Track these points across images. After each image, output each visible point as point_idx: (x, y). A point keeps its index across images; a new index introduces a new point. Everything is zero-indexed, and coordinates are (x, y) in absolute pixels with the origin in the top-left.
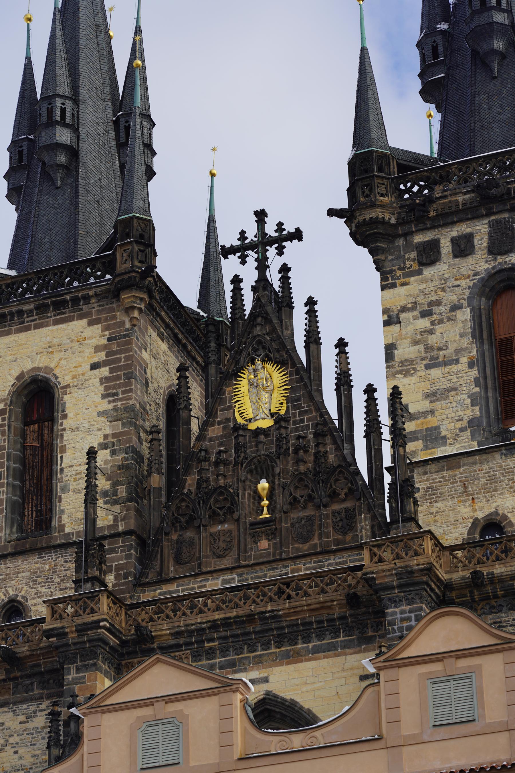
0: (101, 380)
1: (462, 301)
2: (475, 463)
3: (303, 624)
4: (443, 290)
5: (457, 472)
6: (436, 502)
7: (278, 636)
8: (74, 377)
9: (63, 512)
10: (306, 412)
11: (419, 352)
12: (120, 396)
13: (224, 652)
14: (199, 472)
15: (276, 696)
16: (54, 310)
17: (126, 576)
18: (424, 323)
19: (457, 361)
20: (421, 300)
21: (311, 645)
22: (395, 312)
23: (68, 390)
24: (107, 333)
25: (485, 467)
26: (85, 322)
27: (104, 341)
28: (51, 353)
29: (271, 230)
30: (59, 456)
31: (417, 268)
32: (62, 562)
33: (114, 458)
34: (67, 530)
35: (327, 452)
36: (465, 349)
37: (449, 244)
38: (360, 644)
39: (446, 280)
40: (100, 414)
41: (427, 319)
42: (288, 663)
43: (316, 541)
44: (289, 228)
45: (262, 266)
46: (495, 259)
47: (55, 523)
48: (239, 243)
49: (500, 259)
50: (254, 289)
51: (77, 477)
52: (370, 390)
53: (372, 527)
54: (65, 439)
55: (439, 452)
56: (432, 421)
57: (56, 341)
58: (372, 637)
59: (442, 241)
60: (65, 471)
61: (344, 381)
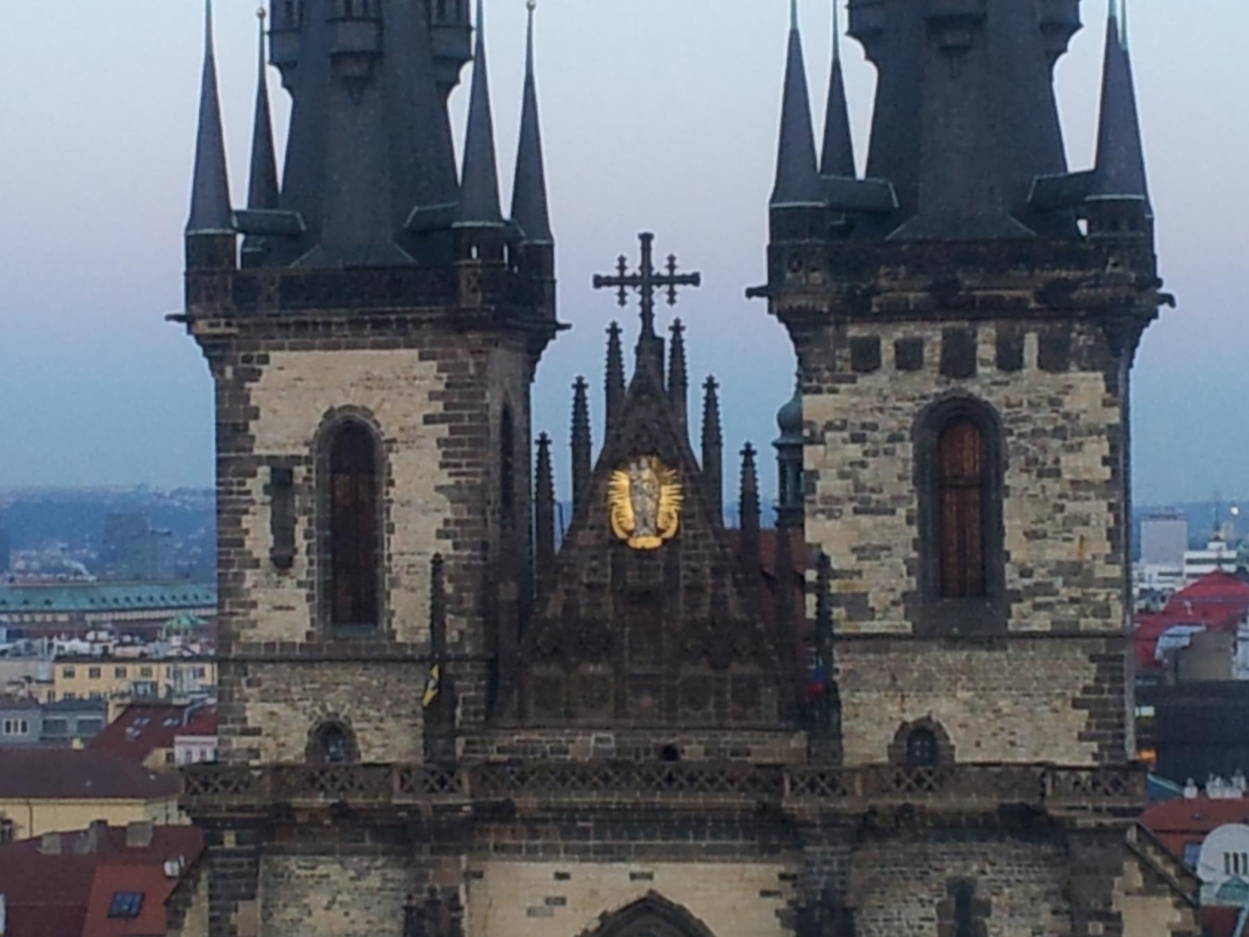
1: (903, 432)
2: (907, 651)
4: (881, 410)
5: (884, 658)
6: (858, 690)
8: (402, 429)
9: (393, 613)
12: (464, 469)
14: (567, 591)
15: (661, 898)
16: (374, 327)
17: (476, 714)
19: (893, 512)
20: (852, 418)
21: (704, 844)
22: (819, 430)
23: (395, 447)
24: (444, 375)
26: (414, 353)
27: (441, 387)
29: (660, 268)
30: (386, 536)
31: (850, 373)
32: (394, 680)
33: (458, 553)
34: (399, 638)
35: (725, 596)
36: (904, 497)
37: (891, 348)
38: (762, 852)
39: (885, 398)
40: (439, 489)
42: (677, 861)
43: (711, 708)
45: (647, 316)
46: (948, 383)
49: (954, 383)
51: (412, 570)
54: (392, 513)
55: (866, 627)
56: (859, 585)
57: (376, 373)
59: (884, 343)
60: (394, 558)
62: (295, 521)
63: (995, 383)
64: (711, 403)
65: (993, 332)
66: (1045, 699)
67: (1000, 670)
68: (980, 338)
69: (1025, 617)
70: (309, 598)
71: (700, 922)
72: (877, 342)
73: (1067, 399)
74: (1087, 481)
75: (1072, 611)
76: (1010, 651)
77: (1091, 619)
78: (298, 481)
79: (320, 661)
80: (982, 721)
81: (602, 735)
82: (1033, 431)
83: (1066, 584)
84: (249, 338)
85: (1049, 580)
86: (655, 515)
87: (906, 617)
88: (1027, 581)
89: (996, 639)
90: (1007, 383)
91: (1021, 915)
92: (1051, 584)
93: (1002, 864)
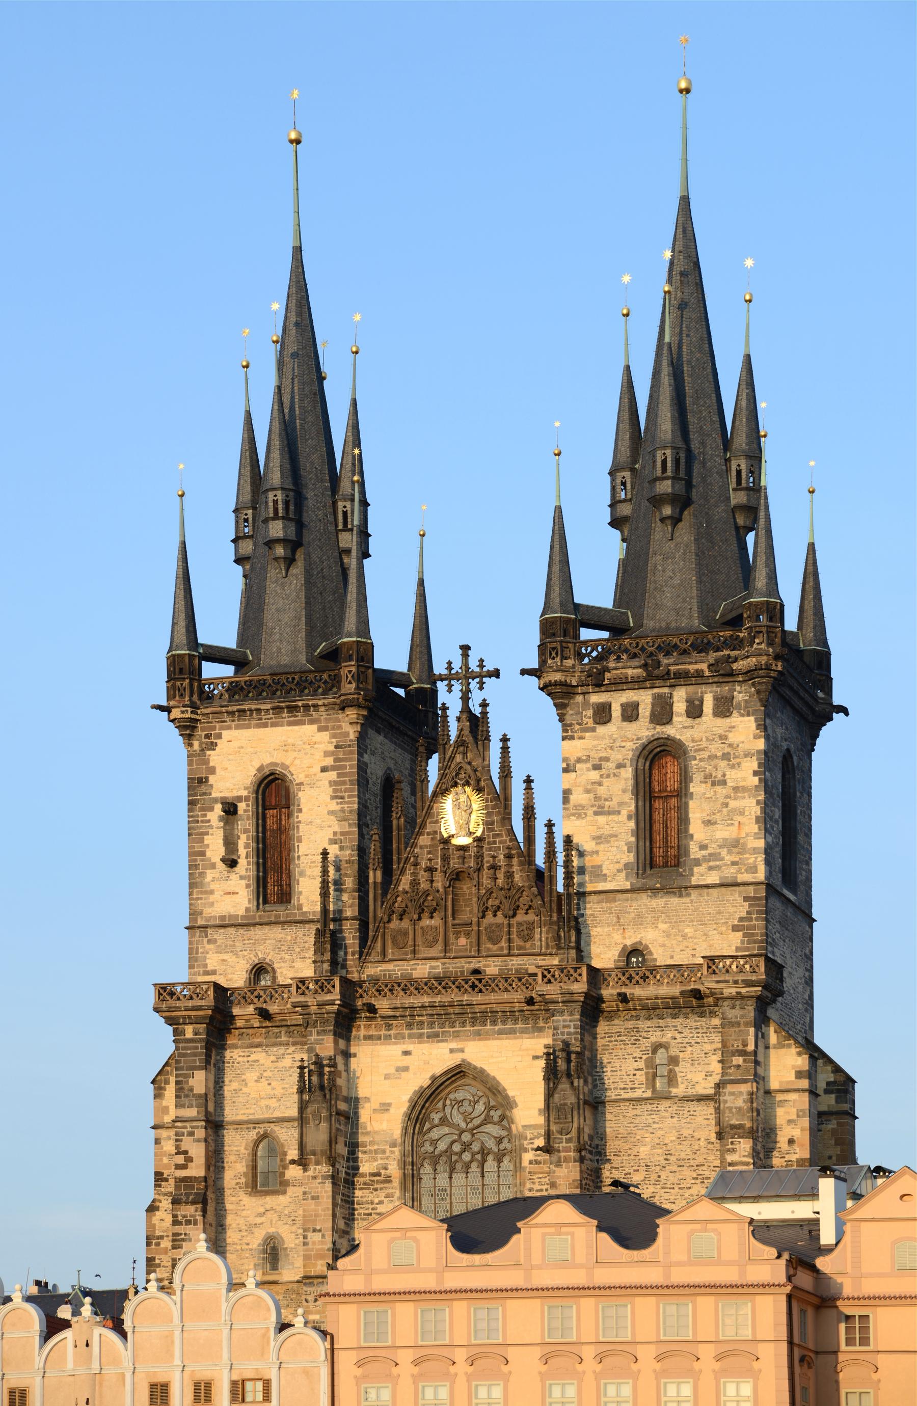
0: (330, 782)
2: (627, 900)
3: (491, 1012)
4: (612, 748)
5: (613, 905)
7: (472, 1018)
8: (307, 776)
9: (301, 893)
10: (498, 835)
11: (590, 800)
12: (346, 800)
13: (431, 1025)
15: (470, 1064)
16: (288, 712)
18: (594, 775)
19: (619, 813)
20: (592, 754)
21: (496, 1028)
22: (572, 762)
24: (334, 740)
25: (634, 904)
26: (315, 727)
28: (287, 751)
33: (342, 852)
34: (305, 909)
37: (619, 708)
38: (533, 1032)
40: (331, 813)
41: (597, 772)
42: (479, 1040)
44: (489, 667)
46: (655, 728)
47: (294, 901)
48: (446, 672)
49: (659, 729)
50: (458, 719)
52: (550, 825)
53: (547, 938)
55: (601, 886)
58: (542, 1027)
59: (613, 705)
61: (529, 813)
62: (239, 838)
63: (685, 727)
64: (505, 750)
65: (684, 693)
66: (715, 926)
67: (686, 910)
68: (675, 699)
69: (702, 875)
70: (248, 886)
71: (494, 1078)
72: (610, 705)
73: (730, 735)
74: (743, 787)
75: (733, 870)
76: (693, 897)
77: (745, 875)
78: (240, 812)
79: (254, 925)
80: (674, 942)
81: (434, 963)
82: (709, 757)
83: (730, 852)
84: (208, 722)
85: (718, 851)
86: (468, 823)
87: (627, 879)
88: (704, 853)
89: (683, 890)
90: (692, 727)
91: (699, 1064)
92: (720, 853)
93: (686, 1032)
